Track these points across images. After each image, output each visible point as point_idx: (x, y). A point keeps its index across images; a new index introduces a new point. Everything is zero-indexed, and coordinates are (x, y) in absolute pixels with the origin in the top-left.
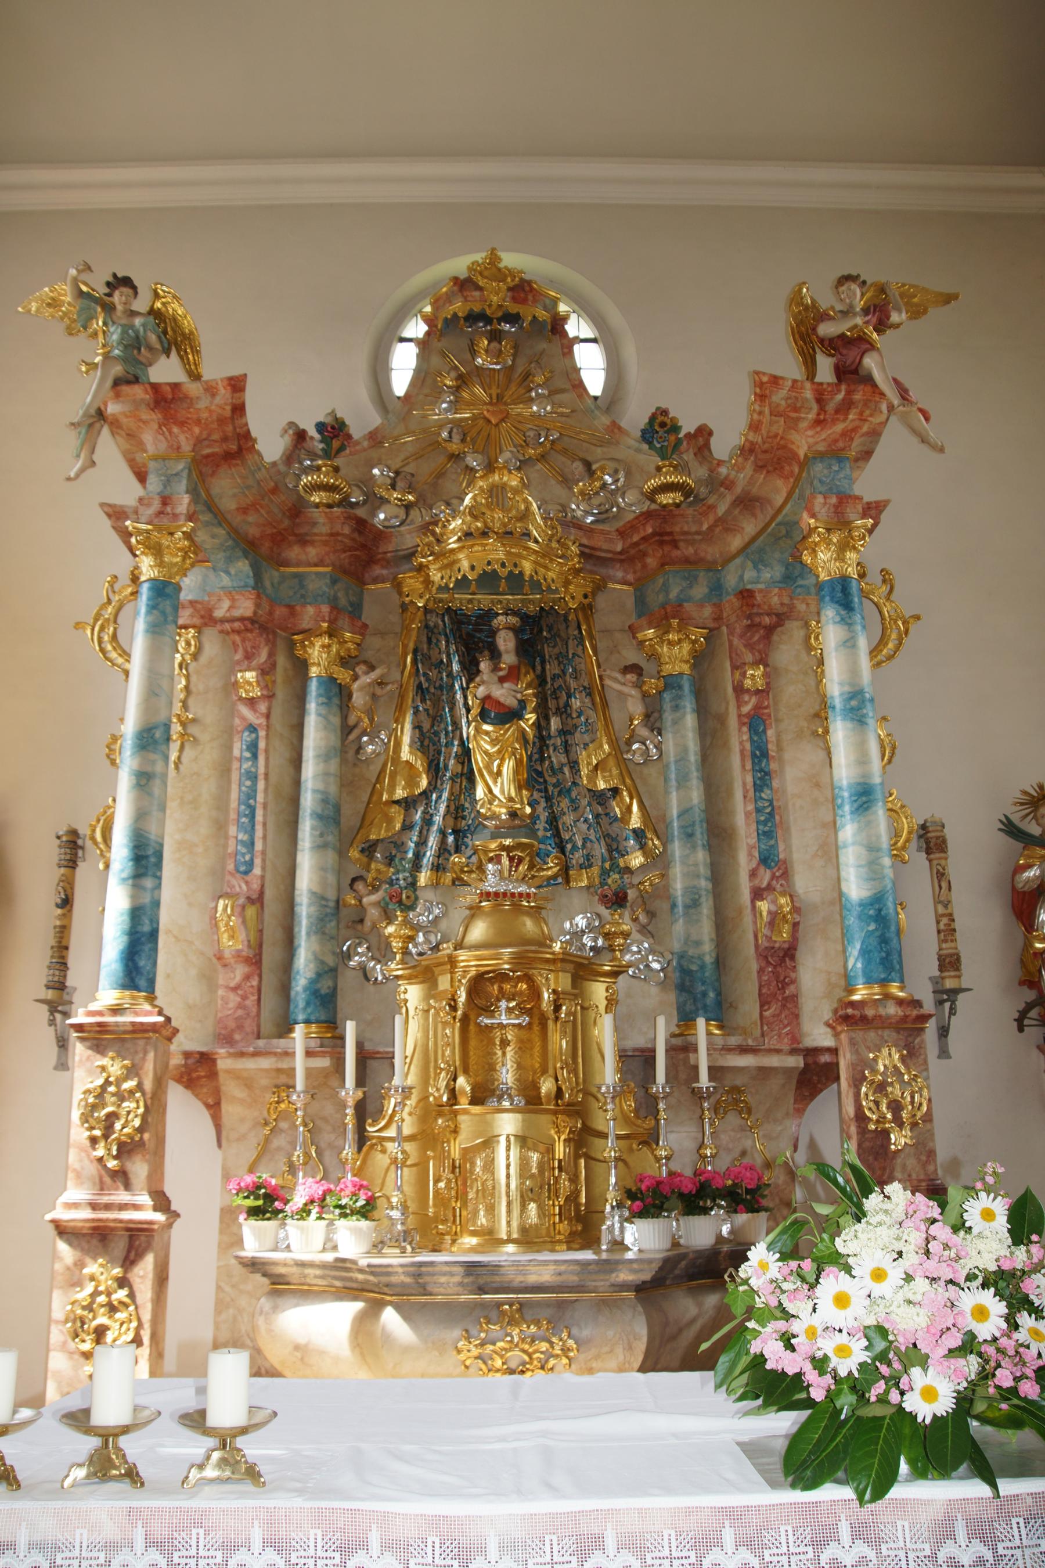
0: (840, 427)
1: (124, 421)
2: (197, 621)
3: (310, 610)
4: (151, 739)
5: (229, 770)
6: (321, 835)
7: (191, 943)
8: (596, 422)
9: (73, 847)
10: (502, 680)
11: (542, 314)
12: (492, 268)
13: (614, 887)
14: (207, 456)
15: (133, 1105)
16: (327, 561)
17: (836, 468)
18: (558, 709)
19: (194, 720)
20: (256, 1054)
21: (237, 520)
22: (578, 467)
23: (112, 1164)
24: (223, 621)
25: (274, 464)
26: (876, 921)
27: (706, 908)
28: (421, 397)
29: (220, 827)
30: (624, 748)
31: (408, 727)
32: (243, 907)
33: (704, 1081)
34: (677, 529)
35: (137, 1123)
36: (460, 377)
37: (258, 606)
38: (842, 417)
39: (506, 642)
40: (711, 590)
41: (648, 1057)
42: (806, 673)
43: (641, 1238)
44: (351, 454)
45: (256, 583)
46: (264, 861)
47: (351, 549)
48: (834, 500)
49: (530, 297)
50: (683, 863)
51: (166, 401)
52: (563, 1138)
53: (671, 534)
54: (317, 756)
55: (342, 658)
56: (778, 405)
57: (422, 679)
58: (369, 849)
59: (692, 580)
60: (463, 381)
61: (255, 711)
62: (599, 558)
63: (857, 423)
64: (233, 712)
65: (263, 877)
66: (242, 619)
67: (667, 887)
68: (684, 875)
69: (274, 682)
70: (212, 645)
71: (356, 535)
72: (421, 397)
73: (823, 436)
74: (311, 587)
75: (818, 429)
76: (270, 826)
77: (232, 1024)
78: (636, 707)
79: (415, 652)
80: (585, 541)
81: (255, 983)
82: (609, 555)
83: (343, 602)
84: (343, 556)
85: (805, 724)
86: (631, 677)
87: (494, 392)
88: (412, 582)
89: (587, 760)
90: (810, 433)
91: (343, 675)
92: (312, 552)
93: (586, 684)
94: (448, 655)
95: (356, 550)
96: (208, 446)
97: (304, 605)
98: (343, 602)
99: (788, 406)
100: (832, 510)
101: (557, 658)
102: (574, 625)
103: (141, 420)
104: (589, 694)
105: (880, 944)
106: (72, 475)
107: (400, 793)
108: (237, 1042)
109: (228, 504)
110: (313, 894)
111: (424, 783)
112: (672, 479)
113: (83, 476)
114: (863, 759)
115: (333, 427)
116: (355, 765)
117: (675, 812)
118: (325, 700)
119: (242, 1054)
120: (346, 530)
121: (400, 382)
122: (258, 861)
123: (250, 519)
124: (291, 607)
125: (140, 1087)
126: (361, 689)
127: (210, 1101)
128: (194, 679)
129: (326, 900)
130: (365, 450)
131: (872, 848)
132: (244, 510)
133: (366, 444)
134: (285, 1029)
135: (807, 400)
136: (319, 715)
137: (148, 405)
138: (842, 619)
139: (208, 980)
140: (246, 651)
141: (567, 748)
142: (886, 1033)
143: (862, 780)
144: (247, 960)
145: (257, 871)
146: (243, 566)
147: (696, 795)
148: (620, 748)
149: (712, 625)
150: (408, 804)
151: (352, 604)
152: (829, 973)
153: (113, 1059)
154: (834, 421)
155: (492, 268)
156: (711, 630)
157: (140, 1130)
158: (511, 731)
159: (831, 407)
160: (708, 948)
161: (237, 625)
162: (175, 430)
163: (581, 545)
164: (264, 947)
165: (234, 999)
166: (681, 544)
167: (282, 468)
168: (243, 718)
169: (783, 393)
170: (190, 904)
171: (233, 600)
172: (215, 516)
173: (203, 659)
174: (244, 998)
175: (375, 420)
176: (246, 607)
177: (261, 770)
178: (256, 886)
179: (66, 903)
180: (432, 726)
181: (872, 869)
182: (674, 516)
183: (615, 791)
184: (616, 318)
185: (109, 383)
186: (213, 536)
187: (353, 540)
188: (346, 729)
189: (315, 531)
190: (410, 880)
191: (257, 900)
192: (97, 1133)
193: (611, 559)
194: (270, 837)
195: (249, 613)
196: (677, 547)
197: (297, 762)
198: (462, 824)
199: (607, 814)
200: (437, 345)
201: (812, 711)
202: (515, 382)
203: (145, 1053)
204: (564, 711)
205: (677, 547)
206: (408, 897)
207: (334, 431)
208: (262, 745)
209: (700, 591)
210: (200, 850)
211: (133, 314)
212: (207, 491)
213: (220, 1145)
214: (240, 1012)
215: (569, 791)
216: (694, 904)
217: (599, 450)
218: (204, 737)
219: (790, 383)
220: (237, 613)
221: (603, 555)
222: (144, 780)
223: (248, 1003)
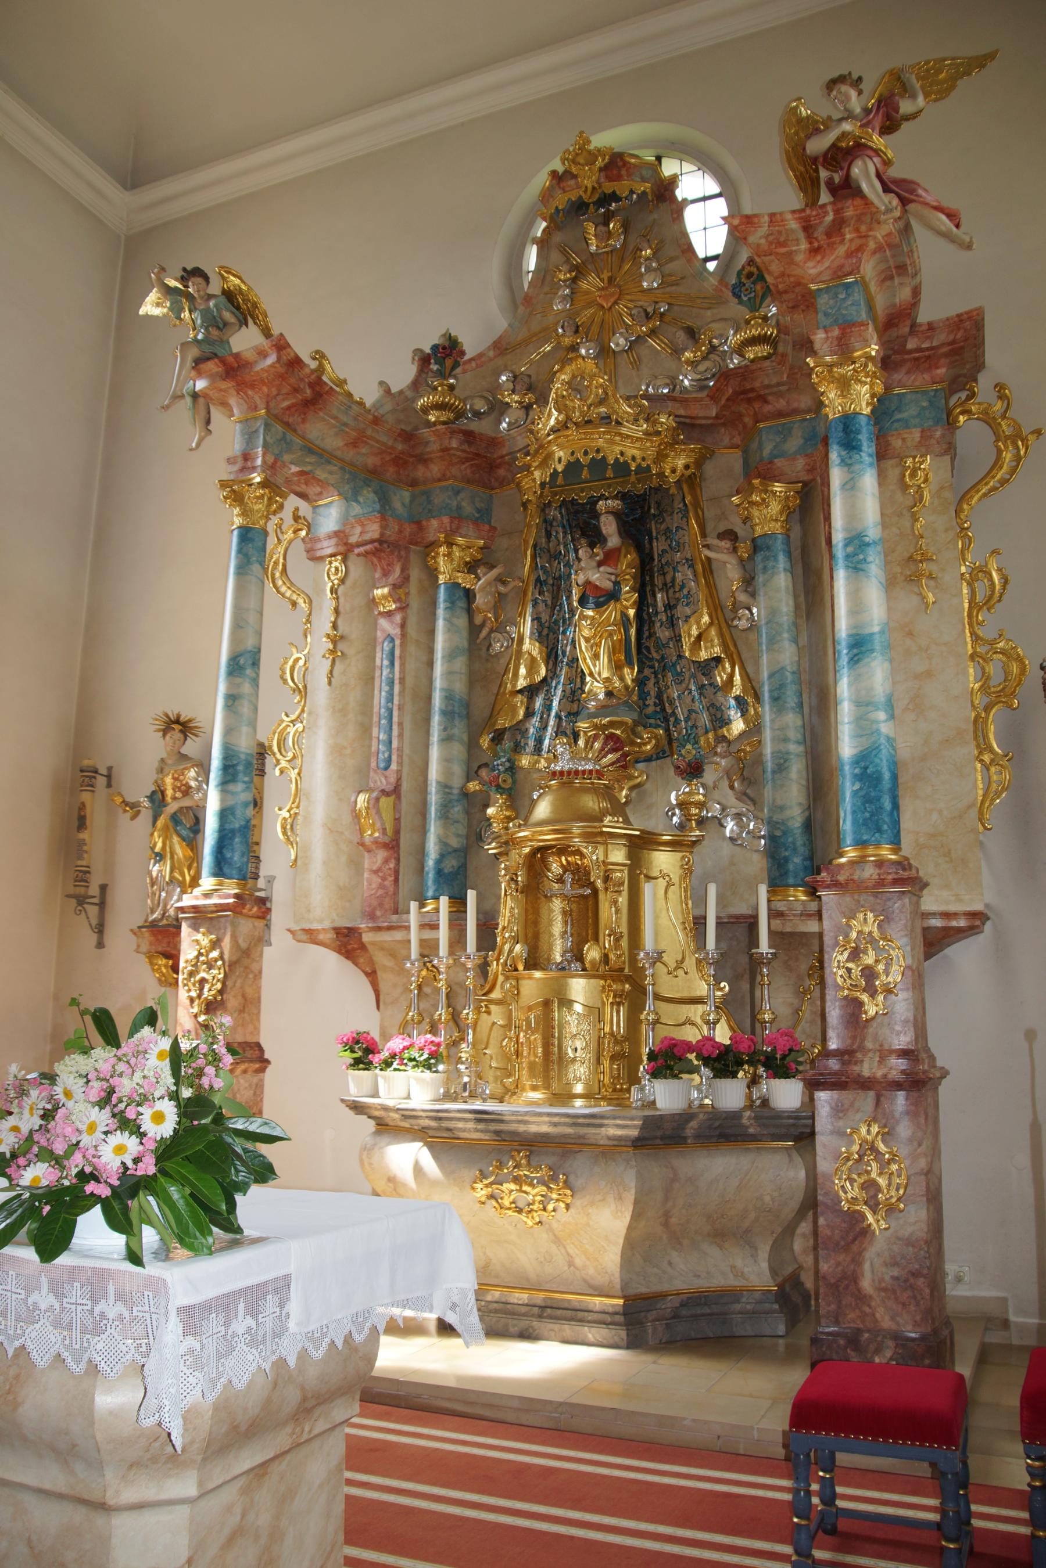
0: (841, 250)
1: (211, 393)
2: (342, 549)
3: (434, 523)
5: (373, 678)
6: (445, 729)
7: (342, 833)
8: (705, 284)
10: (600, 564)
12: (582, 153)
13: (689, 758)
14: (289, 408)
15: (216, 971)
16: (448, 475)
17: (842, 296)
18: (665, 584)
19: (342, 637)
20: (389, 928)
21: (349, 455)
22: (681, 336)
23: (202, 1018)
24: (359, 545)
25: (401, 392)
26: (860, 780)
28: (542, 296)
29: (365, 730)
30: (731, 615)
31: (529, 619)
32: (377, 799)
33: (764, 946)
34: (757, 384)
35: (219, 986)
37: (384, 527)
38: (837, 239)
39: (609, 527)
40: (806, 440)
41: (751, 923)
42: (900, 515)
44: (477, 366)
45: (383, 506)
46: (400, 756)
47: (467, 460)
48: (836, 332)
49: (624, 172)
50: (772, 729)
52: (611, 1000)
53: (752, 390)
54: (443, 657)
55: (467, 563)
56: (758, 245)
57: (541, 573)
58: (498, 737)
59: (785, 433)
60: (579, 272)
61: (392, 622)
62: (701, 426)
63: (858, 242)
64: (375, 626)
65: (399, 772)
66: (372, 541)
67: (761, 755)
68: (773, 740)
69: (407, 594)
70: (358, 568)
71: (465, 447)
72: (542, 296)
73: (827, 264)
74: (436, 501)
75: (819, 258)
76: (407, 725)
77: (375, 903)
79: (535, 546)
80: (682, 412)
81: (392, 866)
82: (709, 422)
83: (468, 509)
84: (463, 467)
85: (898, 570)
86: (726, 544)
87: (606, 275)
88: (526, 484)
90: (810, 264)
91: (465, 580)
92: (435, 469)
93: (689, 556)
94: (566, 546)
95: (473, 459)
96: (284, 400)
97: (428, 520)
98: (468, 509)
99: (771, 243)
100: (835, 343)
101: (665, 534)
102: (678, 498)
103: (221, 390)
104: (692, 566)
105: (864, 804)
106: (194, 445)
107: (521, 683)
108: (378, 918)
109: (333, 443)
110: (438, 782)
111: (543, 672)
112: (755, 332)
113: (203, 444)
114: (857, 608)
115: (444, 348)
116: (487, 660)
117: (765, 675)
118: (448, 605)
119: (379, 929)
120: (454, 444)
122: (394, 758)
123: (364, 451)
124: (418, 523)
125: (221, 957)
126: (483, 589)
127: (368, 969)
128: (341, 600)
129: (451, 788)
130: (491, 360)
131: (863, 704)
132: (354, 444)
133: (491, 354)
135: (792, 231)
136: (445, 619)
137: (221, 376)
138: (843, 461)
139: (355, 865)
140: (383, 569)
141: (672, 623)
142: (863, 898)
143: (854, 631)
144: (386, 846)
145: (394, 766)
146: (368, 495)
149: (805, 478)
150: (531, 691)
151: (479, 511)
152: (918, 833)
153: (204, 934)
154: (831, 246)
155: (582, 153)
156: (805, 484)
157: (221, 992)
158: (611, 612)
159: (819, 233)
160: (795, 816)
161: (368, 547)
162: (250, 392)
163: (676, 416)
164: (402, 833)
165: (376, 880)
166: (770, 398)
167: (409, 394)
168: (383, 631)
169: (764, 230)
170: (340, 800)
171: (363, 525)
172: (321, 456)
173: (349, 582)
174: (384, 879)
176: (374, 530)
177: (397, 675)
178: (393, 780)
180: (551, 616)
181: (863, 725)
182: (753, 372)
183: (718, 660)
184: (733, 167)
185: (189, 363)
186: (331, 473)
187: (463, 451)
188: (474, 630)
189: (428, 449)
190: (508, 765)
191: (395, 791)
192: (194, 994)
193: (712, 425)
194: (407, 734)
195: (376, 536)
196: (766, 402)
197: (430, 664)
199: (711, 685)
200: (558, 238)
201: (906, 555)
202: (618, 264)
203: (225, 928)
205: (766, 402)
206: (504, 781)
208: (397, 653)
209: (794, 443)
210: (348, 751)
211: (210, 297)
212: (303, 438)
213: (378, 1007)
214: (380, 892)
215: (674, 665)
216: (781, 767)
217: (709, 313)
218: (351, 651)
219: (767, 219)
220: (367, 537)
221: (703, 422)
223: (387, 883)
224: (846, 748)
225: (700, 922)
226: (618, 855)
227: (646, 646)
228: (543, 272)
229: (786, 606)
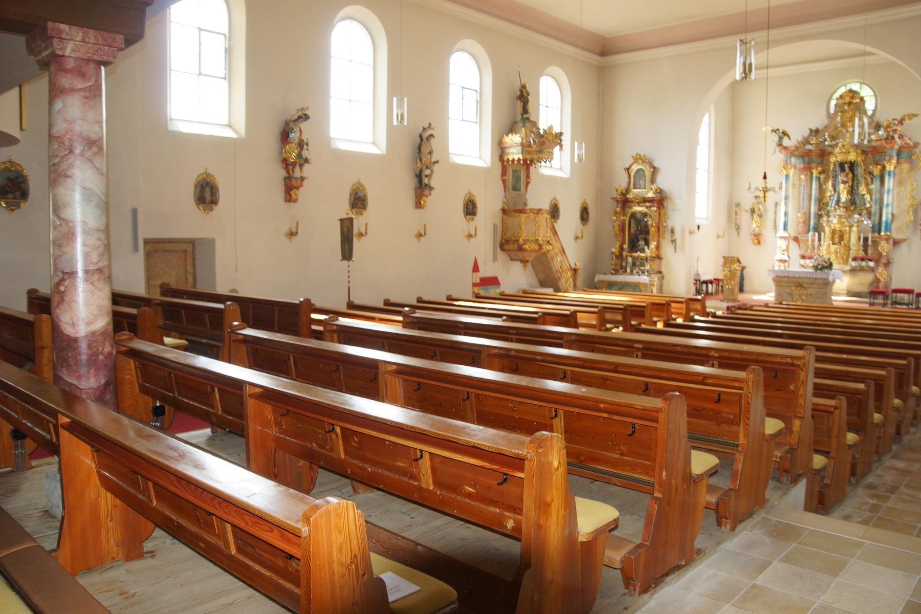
4: (786, 198)
9: (776, 204)
11: (858, 100)
27: (878, 215)
36: (842, 112)
43: (854, 264)
51: (785, 148)
78: (869, 180)
89: (861, 188)
121: (832, 110)
131: (887, 213)
134: (809, 231)
139: (798, 226)
147: (878, 196)
148: (867, 185)
175: (826, 122)
176: (802, 166)
179: (776, 213)
181: (887, 217)
191: (805, 214)
198: (838, 201)
204: (858, 180)
207: (817, 131)
222: (786, 204)
224: (884, 219)
225: (859, 238)
226: (847, 229)
227: (852, 191)
228: (836, 112)
229: (878, 187)
